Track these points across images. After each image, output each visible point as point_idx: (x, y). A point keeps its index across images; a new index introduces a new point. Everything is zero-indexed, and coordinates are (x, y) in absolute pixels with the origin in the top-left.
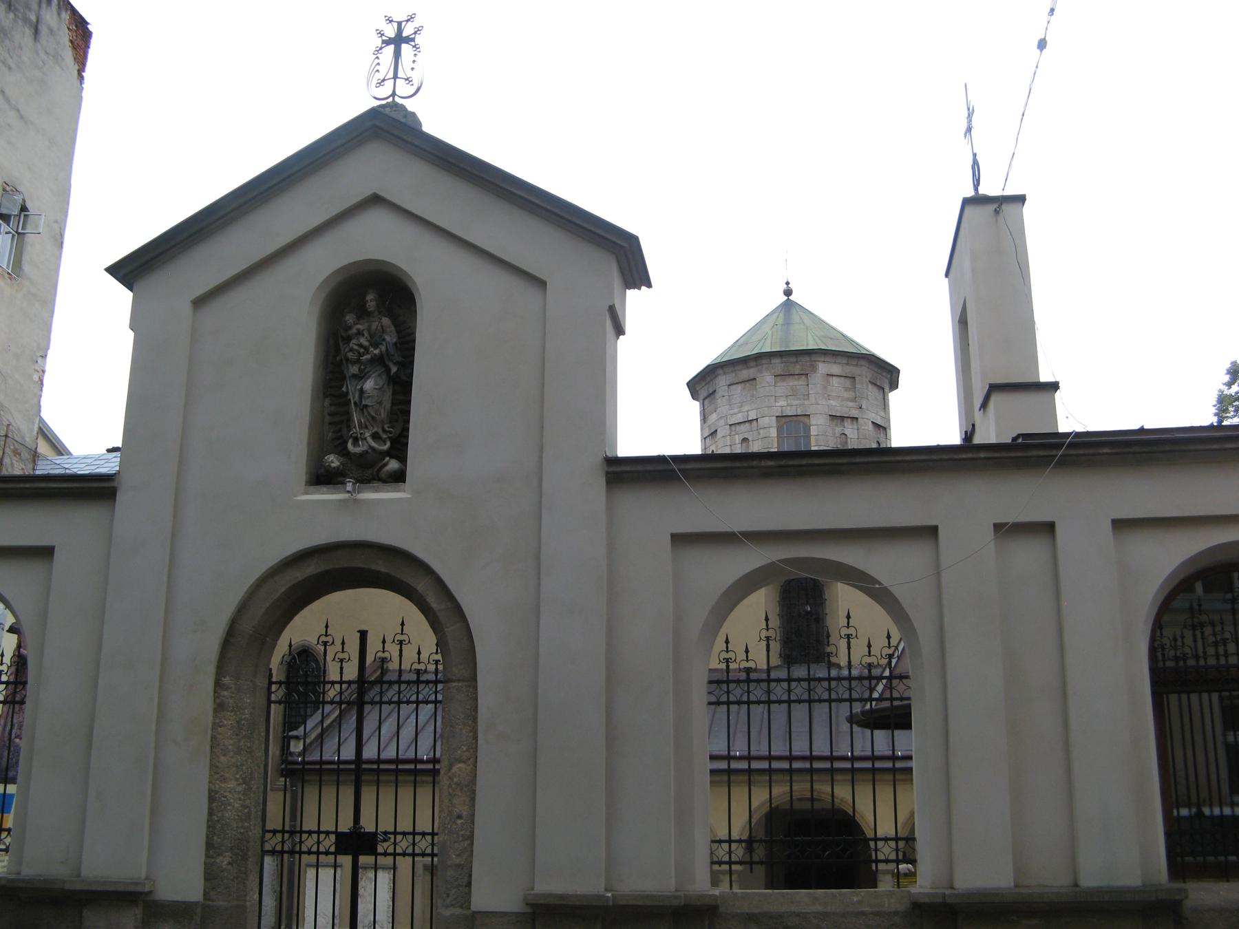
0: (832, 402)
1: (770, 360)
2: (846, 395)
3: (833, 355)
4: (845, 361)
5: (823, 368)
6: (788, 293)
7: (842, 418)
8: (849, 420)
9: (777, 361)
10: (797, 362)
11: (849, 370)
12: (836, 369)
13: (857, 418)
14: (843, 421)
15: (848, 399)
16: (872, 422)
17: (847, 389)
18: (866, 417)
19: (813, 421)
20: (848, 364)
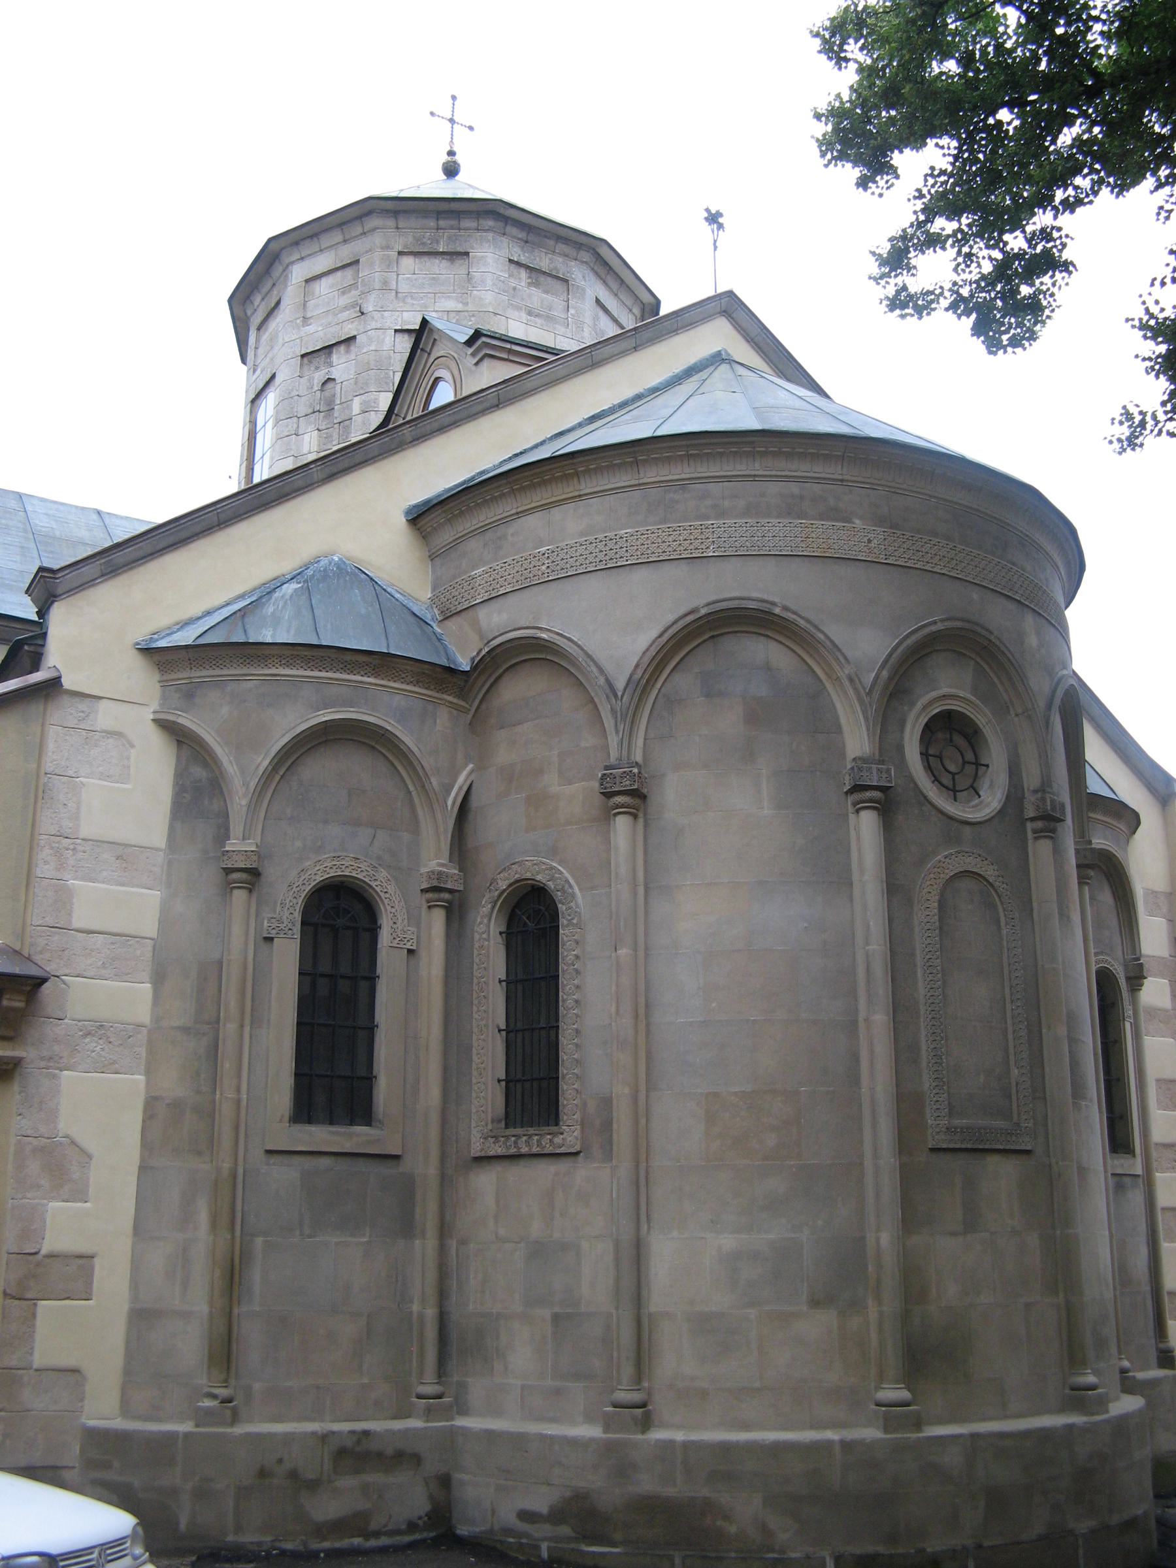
0: (311, 329)
1: (252, 303)
2: (344, 300)
3: (311, 237)
4: (337, 236)
5: (298, 273)
6: (451, 170)
7: (328, 349)
8: (342, 348)
9: (257, 299)
10: (274, 285)
11: (346, 253)
12: (323, 262)
13: (354, 338)
14: (330, 353)
15: (346, 308)
16: (396, 331)
17: (344, 291)
18: (374, 325)
19: (278, 380)
20: (345, 241)
